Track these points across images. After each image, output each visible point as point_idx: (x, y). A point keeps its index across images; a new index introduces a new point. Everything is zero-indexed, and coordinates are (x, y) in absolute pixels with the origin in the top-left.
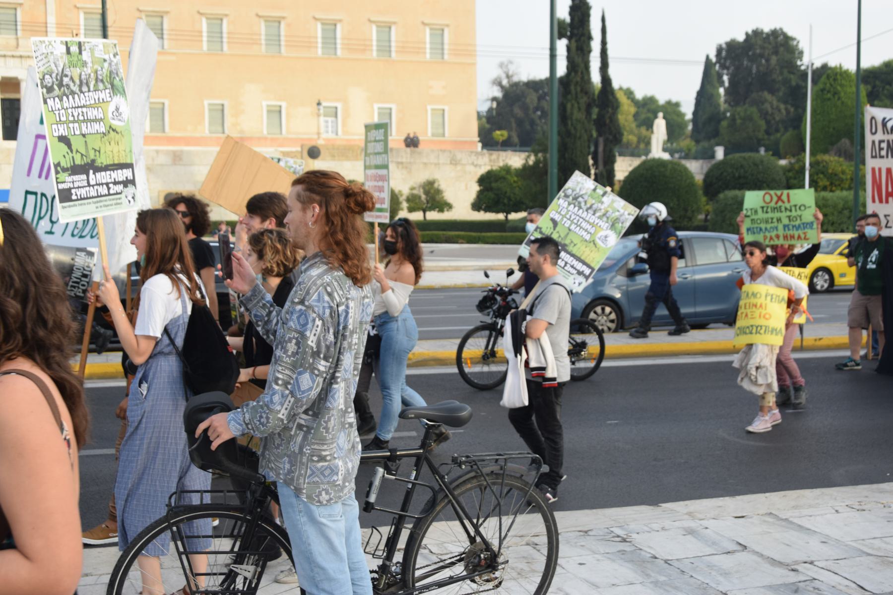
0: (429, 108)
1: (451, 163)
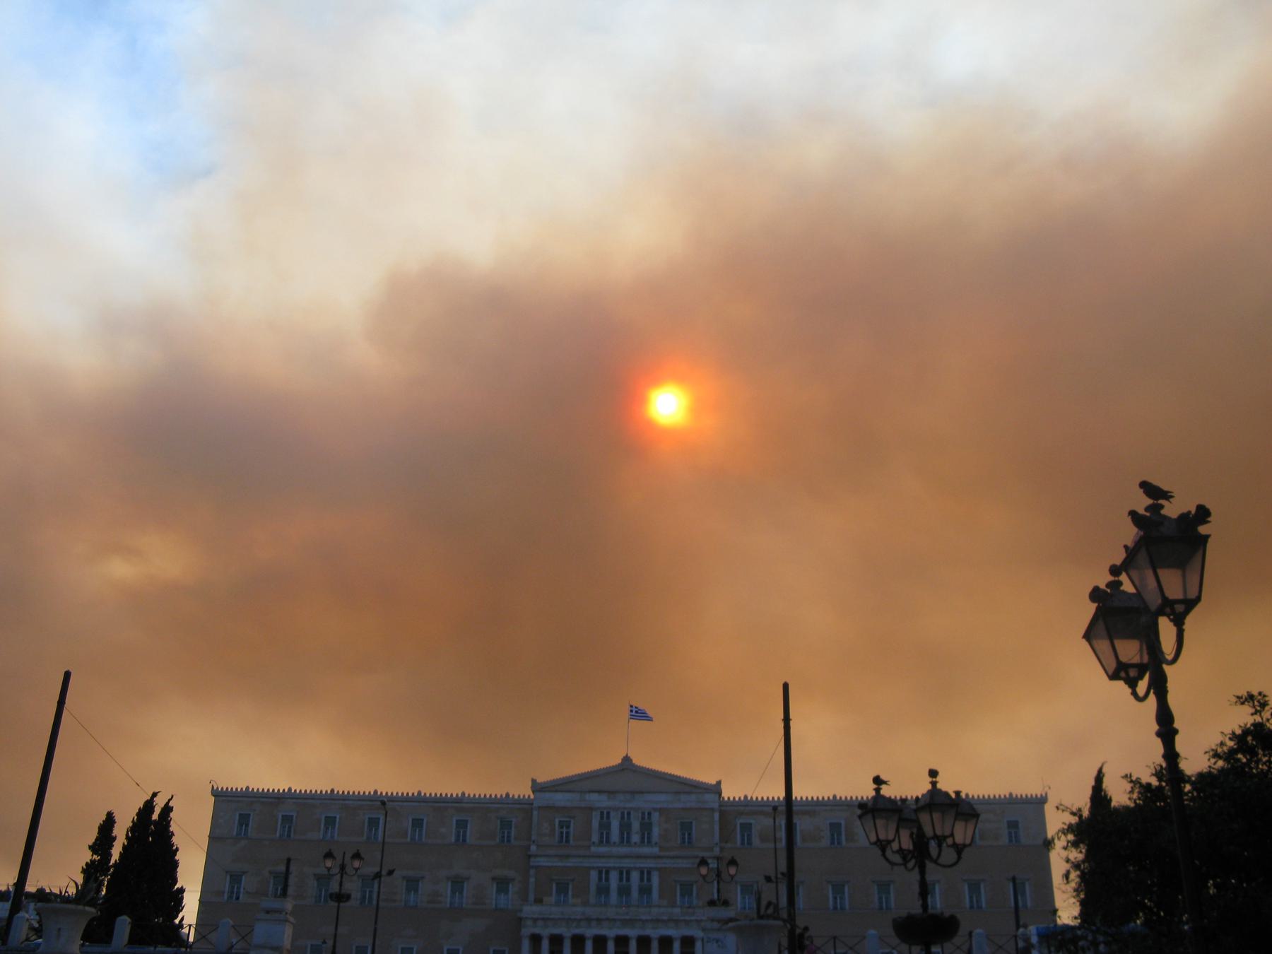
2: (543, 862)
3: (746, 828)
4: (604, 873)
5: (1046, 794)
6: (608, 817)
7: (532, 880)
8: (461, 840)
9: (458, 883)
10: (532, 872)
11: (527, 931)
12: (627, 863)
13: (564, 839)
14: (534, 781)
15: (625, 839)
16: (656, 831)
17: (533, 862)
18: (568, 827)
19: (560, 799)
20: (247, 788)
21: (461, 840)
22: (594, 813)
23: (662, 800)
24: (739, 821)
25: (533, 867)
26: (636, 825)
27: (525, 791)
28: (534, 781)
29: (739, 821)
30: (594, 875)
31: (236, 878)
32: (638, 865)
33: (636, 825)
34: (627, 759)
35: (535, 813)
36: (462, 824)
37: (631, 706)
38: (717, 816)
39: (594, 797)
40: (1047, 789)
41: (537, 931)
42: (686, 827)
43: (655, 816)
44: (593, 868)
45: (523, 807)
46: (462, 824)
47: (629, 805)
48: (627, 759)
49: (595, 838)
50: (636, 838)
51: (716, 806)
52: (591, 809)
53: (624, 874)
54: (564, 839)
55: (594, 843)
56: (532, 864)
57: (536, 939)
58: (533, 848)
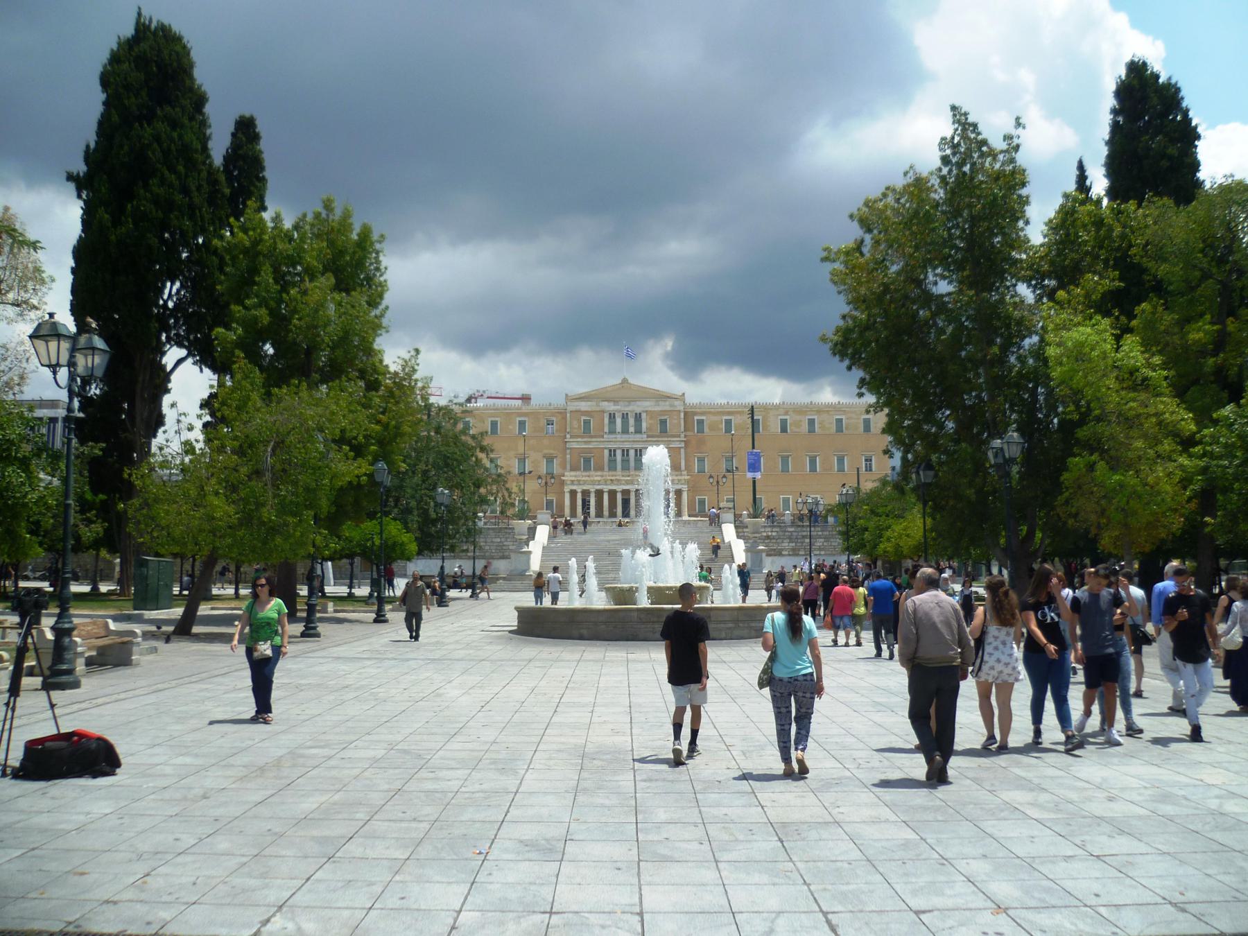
2: (575, 446)
3: (701, 422)
4: (612, 453)
7: (568, 456)
10: (568, 451)
11: (567, 489)
12: (627, 446)
15: (625, 431)
16: (644, 425)
17: (568, 445)
19: (584, 406)
23: (648, 405)
24: (696, 418)
29: (696, 418)
30: (606, 452)
34: (625, 381)
36: (522, 424)
38: (682, 415)
41: (574, 488)
42: (663, 423)
43: (644, 415)
45: (562, 413)
46: (522, 424)
49: (606, 430)
50: (632, 429)
51: (682, 408)
52: (603, 412)
57: (573, 493)
58: (568, 436)
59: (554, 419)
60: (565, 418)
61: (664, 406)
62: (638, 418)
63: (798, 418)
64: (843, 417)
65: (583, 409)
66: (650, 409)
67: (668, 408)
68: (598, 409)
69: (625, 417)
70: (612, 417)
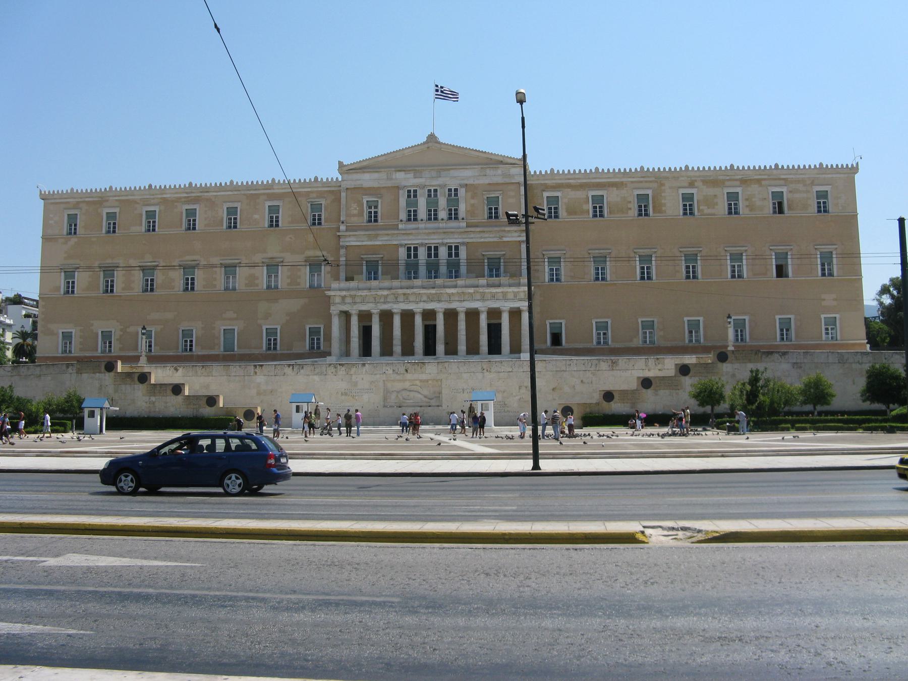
0: (823, 316)
1: (839, 362)
5: (857, 164)
6: (415, 196)
8: (274, 223)
9: (272, 267)
10: (343, 251)
13: (373, 218)
14: (340, 163)
16: (462, 208)
18: (376, 207)
19: (367, 180)
20: (72, 189)
21: (274, 223)
22: (401, 192)
23: (468, 175)
24: (546, 194)
25: (343, 247)
26: (442, 202)
27: (331, 173)
28: (340, 163)
29: (546, 194)
31: (69, 274)
32: (445, 241)
33: (442, 202)
34: (432, 138)
35: (343, 195)
37: (437, 86)
39: (400, 175)
40: (858, 159)
43: (462, 192)
44: (401, 245)
46: (274, 210)
47: (435, 182)
48: (432, 138)
49: (403, 215)
52: (398, 188)
53: (433, 251)
54: (373, 218)
55: (401, 221)
56: (341, 244)
57: (346, 315)
58: (343, 227)
59: (323, 202)
60: (338, 200)
61: (495, 176)
62: (453, 195)
63: (711, 191)
64: (784, 189)
65: (366, 185)
66: (470, 182)
67: (499, 180)
68: (389, 184)
69: (432, 195)
70: (412, 195)
